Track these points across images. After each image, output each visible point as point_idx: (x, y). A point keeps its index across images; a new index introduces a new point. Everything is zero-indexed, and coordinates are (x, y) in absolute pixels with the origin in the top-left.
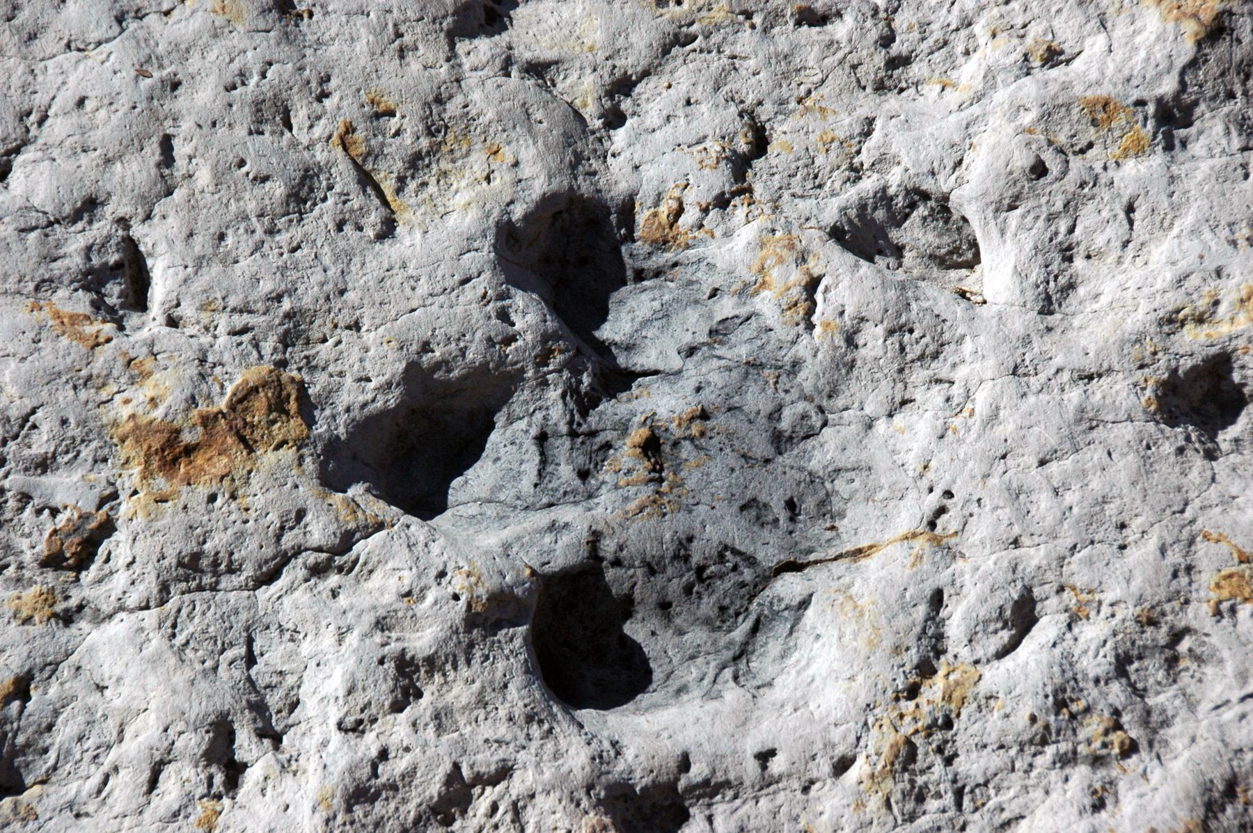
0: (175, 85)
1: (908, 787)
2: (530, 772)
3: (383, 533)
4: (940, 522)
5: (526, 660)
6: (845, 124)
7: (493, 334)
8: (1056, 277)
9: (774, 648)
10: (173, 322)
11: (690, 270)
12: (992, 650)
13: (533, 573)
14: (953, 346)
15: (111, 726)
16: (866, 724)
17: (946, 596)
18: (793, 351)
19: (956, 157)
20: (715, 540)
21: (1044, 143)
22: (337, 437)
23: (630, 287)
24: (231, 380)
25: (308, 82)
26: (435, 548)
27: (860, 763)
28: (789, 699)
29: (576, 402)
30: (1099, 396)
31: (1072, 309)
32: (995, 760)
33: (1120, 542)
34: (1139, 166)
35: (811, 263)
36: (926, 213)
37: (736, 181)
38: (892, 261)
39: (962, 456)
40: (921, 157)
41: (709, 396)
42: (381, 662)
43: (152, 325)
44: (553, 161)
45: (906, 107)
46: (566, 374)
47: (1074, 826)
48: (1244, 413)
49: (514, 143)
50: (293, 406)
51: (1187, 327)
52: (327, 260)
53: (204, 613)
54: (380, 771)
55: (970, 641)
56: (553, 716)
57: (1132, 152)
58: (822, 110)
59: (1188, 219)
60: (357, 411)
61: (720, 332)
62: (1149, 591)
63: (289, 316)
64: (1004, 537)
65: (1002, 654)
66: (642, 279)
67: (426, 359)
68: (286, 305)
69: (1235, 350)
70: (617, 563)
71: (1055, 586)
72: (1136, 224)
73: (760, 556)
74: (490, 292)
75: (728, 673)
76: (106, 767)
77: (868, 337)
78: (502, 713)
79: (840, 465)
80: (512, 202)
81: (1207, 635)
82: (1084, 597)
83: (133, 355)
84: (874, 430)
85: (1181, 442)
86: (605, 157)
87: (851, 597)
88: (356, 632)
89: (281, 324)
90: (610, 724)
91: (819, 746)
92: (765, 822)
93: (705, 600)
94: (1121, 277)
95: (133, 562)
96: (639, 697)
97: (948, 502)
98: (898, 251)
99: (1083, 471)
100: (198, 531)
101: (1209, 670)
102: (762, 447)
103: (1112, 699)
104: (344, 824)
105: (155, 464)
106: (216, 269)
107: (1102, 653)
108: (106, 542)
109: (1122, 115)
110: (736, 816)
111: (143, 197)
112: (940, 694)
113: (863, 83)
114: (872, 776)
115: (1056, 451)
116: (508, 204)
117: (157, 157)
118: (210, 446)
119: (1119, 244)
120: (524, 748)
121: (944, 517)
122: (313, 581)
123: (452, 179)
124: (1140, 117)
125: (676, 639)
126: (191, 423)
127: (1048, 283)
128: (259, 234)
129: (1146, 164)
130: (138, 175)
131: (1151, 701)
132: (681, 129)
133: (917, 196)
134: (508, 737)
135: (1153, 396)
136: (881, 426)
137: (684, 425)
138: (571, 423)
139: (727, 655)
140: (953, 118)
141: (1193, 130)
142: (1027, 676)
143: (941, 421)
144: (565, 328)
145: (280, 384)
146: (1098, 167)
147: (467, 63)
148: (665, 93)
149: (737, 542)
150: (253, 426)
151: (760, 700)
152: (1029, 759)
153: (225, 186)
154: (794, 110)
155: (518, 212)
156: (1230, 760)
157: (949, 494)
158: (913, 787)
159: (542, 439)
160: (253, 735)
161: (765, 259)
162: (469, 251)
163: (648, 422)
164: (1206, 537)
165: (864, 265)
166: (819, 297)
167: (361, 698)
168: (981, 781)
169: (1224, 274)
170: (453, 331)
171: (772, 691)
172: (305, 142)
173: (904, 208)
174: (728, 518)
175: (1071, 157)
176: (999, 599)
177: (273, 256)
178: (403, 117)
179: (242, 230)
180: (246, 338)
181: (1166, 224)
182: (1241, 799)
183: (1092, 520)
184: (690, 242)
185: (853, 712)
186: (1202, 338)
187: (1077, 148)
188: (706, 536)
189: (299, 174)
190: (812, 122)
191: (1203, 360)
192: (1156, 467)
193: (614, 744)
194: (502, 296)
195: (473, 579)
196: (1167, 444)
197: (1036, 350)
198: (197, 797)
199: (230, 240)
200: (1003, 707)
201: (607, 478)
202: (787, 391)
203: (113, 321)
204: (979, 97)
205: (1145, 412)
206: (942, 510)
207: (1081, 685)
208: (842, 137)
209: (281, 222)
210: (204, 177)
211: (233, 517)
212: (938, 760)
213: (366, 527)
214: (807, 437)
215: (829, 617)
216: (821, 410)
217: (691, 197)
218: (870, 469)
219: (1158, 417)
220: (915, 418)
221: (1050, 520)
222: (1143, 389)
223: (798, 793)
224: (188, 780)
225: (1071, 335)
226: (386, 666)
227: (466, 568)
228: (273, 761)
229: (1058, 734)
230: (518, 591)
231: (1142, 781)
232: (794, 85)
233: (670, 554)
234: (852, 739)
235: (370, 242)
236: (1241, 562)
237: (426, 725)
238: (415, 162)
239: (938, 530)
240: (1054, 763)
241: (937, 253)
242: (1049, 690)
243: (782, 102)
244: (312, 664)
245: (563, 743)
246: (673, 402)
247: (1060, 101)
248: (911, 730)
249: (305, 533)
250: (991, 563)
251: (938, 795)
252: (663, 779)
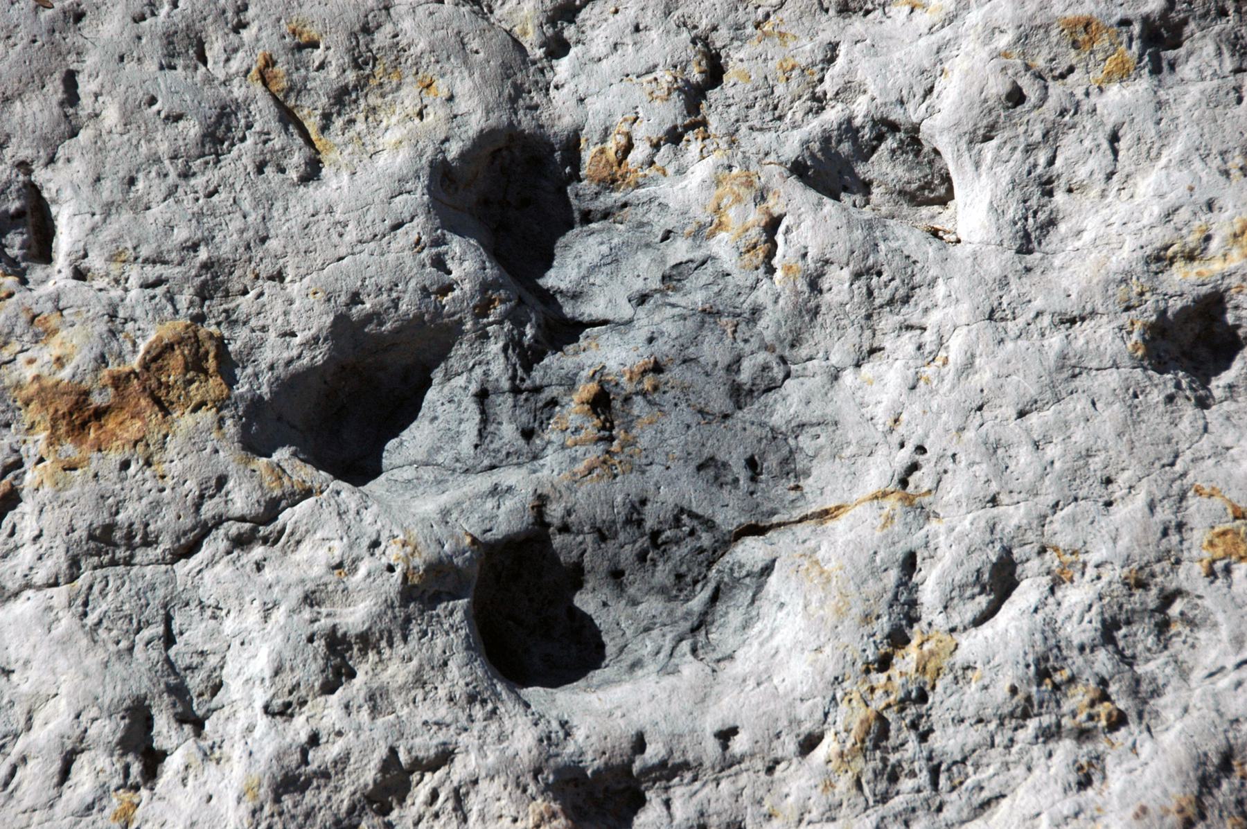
0: (79, 17)
1: (880, 765)
2: (473, 756)
3: (311, 500)
4: (912, 480)
5: (467, 636)
6: (807, 50)
7: (427, 283)
8: (1035, 213)
9: (735, 617)
10: (80, 275)
11: (641, 210)
12: (969, 617)
13: (474, 541)
14: (924, 290)
15: (19, 713)
16: (834, 698)
17: (919, 560)
18: (752, 297)
19: (926, 84)
20: (671, 501)
21: (1021, 68)
22: (261, 397)
23: (577, 230)
24: (144, 337)
25: (224, 12)
26: (368, 516)
27: (829, 738)
28: (751, 673)
29: (519, 356)
30: (1081, 341)
31: (1052, 247)
32: (972, 735)
33: (1106, 498)
34: (1124, 92)
35: (771, 201)
36: (895, 145)
37: (689, 114)
38: (858, 198)
39: (935, 408)
40: (889, 85)
41: (662, 348)
42: (311, 639)
43: (57, 277)
44: (491, 94)
45: (872, 30)
46: (507, 326)
47: (1059, 805)
48: (1238, 357)
49: (448, 76)
50: (211, 364)
51: (1176, 265)
52: (246, 205)
53: (118, 590)
54: (310, 757)
55: (946, 607)
56: (497, 695)
57: (1116, 77)
58: (782, 35)
59: (1177, 148)
60: (281, 369)
61: (673, 278)
62: (1137, 551)
63: (206, 266)
64: (981, 495)
65: (979, 621)
66: (591, 222)
67: (356, 311)
68: (203, 254)
69: (1228, 289)
70: (565, 529)
71: (1036, 547)
72: (1121, 154)
73: (719, 519)
74: (424, 238)
75: (685, 646)
76: (13, 758)
77: (834, 282)
78: (442, 692)
79: (804, 419)
80: (447, 140)
81: (1200, 597)
82: (1068, 558)
83: (36, 310)
84: (840, 381)
85: (1171, 389)
86: (547, 90)
87: (817, 562)
88: (283, 608)
89: (198, 275)
90: (559, 703)
91: (782, 724)
92: (726, 806)
93: (660, 567)
94: (1105, 212)
95: (40, 535)
96: (591, 674)
97: (920, 458)
98: (865, 187)
99: (1066, 422)
100: (111, 500)
101: (1202, 635)
102: (719, 401)
103: (1098, 667)
104: (272, 815)
105: (63, 429)
106: (126, 216)
107: (1087, 619)
108: (10, 515)
109: (1105, 36)
110: (695, 800)
111: (45, 139)
112: (913, 665)
113: (826, 5)
114: (841, 755)
115: (1036, 402)
116: (443, 142)
117: (60, 95)
118: (122, 408)
119: (1102, 176)
120: (466, 730)
121: (917, 474)
122: (235, 554)
123: (382, 115)
124: (1125, 38)
125: (630, 610)
126: (100, 383)
127: (1026, 219)
128: (173, 177)
129: (1132, 88)
130: (39, 115)
131: (1140, 669)
132: (630, 58)
133: (885, 126)
134: (448, 719)
135: (1140, 341)
136: (848, 377)
137: (636, 379)
138: (513, 378)
139: (685, 626)
140: (923, 42)
141: (1182, 51)
142: (1006, 644)
143: (913, 370)
144: (508, 278)
145: (197, 341)
146: (1079, 94)
148: (611, 19)
149: (694, 504)
150: (168, 386)
151: (721, 676)
152: (1009, 734)
153: (134, 126)
154: (752, 36)
155: (454, 150)
156: (1226, 731)
157: (921, 449)
158: (885, 766)
159: (482, 396)
160: (172, 721)
161: (721, 198)
162: (401, 193)
163: (597, 377)
164: (1199, 492)
165: (829, 205)
166: (779, 238)
167: (288, 679)
168: (959, 758)
169: (1216, 205)
170: (385, 281)
171: (734, 664)
172: (222, 77)
173: (871, 140)
174: (684, 478)
175: (1050, 83)
176: (976, 562)
177: (188, 201)
178: (328, 48)
179: (153, 174)
180: (160, 291)
181: (1153, 153)
182: (1238, 773)
183: (1074, 475)
184: (640, 180)
185: (821, 686)
186: (1193, 277)
187: (1057, 73)
188: (661, 498)
189: (215, 112)
190: (772, 48)
191: (1194, 301)
192: (1144, 416)
193: (563, 724)
194: (437, 242)
195: (409, 549)
196: (1156, 391)
197: (1014, 292)
198: (112, 788)
199: (140, 185)
200: (982, 677)
201: (553, 437)
202: (746, 341)
203: (14, 274)
204: (951, 19)
205: (1132, 357)
206: (914, 467)
207: (1065, 653)
208: (804, 64)
209: (196, 165)
210: (111, 116)
211: (148, 485)
212: (912, 736)
213: (293, 494)
214: (768, 390)
215: (793, 584)
216: (783, 360)
217: (641, 133)
218: (836, 423)
219: (1146, 363)
220: (884, 367)
221: (1030, 476)
222: (1130, 333)
223: (762, 774)
224: (102, 770)
225: (1051, 275)
226: (315, 644)
227: (401, 537)
228: (194, 749)
229: (1041, 706)
230: (458, 561)
231: (1131, 755)
232: (751, 8)
233: (621, 519)
234: (819, 715)
235: (294, 185)
236: (1236, 518)
237: (360, 707)
238: (342, 97)
239: (911, 489)
240: (1037, 737)
241: (907, 188)
242: (1030, 659)
243: (739, 27)
244: (237, 642)
245: (508, 724)
246: (624, 354)
247: (1038, 22)
248: (883, 705)
249: (226, 502)
250: (967, 523)
251: (913, 774)
252: (617, 761)
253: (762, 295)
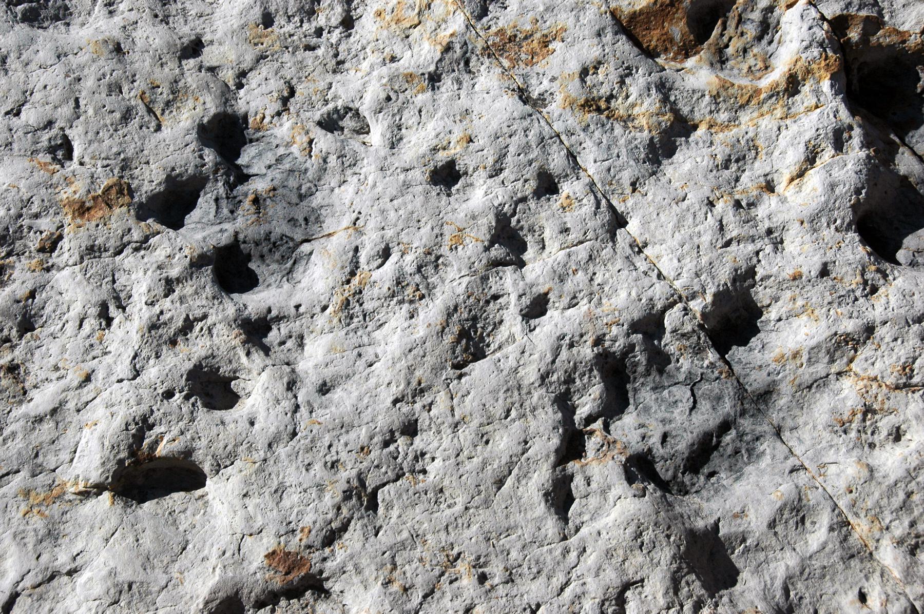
9: (301, 269)
13: (214, 247)
26: (178, 240)
27: (331, 306)
35: (310, 134)
41: (276, 182)
50: (126, 192)
52: (136, 140)
61: (279, 160)
63: (123, 160)
65: (378, 267)
68: (122, 156)
70: (244, 242)
73: (295, 238)
75: (285, 279)
78: (204, 296)
101: (449, 269)
102: (295, 199)
106: (96, 144)
128: (111, 131)
136: (337, 190)
139: (285, 272)
147: (186, 68)
155: (205, 120)
159: (217, 200)
166: (313, 146)
167: (153, 294)
170: (183, 163)
176: (377, 248)
180: (108, 168)
183: (408, 219)
193: (244, 305)
199: (101, 134)
206: (358, 219)
210: (91, 112)
216: (315, 186)
217: (267, 113)
230: (209, 254)
238: (168, 104)
245: (226, 306)
253: (308, 165)
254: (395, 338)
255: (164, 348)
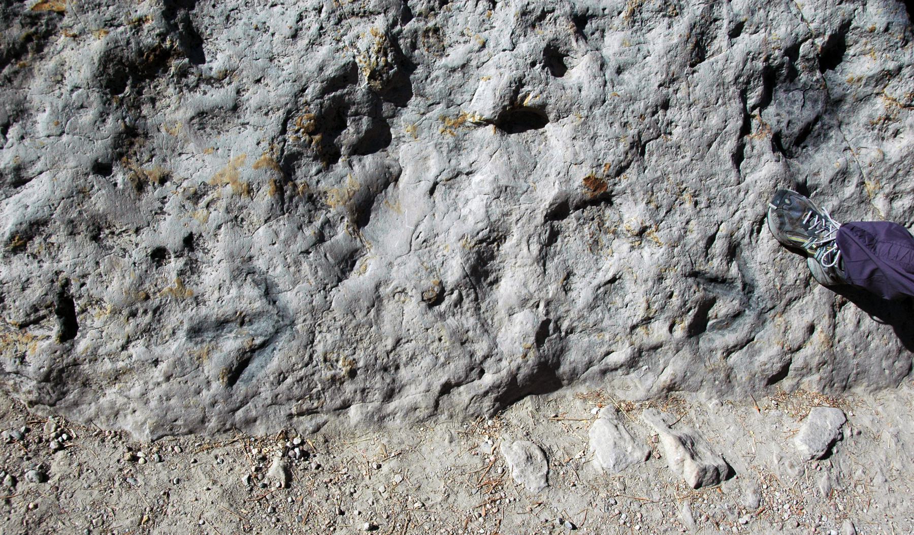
32: (650, 15)
254: (660, 40)
255: (529, 29)
